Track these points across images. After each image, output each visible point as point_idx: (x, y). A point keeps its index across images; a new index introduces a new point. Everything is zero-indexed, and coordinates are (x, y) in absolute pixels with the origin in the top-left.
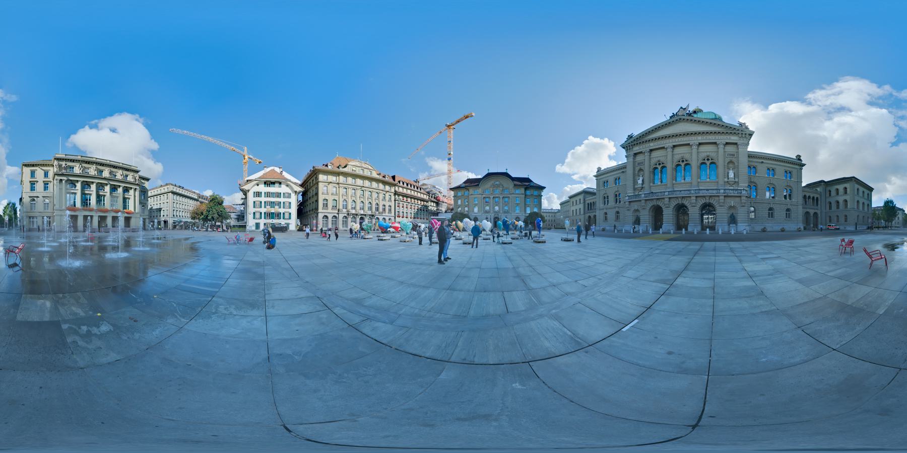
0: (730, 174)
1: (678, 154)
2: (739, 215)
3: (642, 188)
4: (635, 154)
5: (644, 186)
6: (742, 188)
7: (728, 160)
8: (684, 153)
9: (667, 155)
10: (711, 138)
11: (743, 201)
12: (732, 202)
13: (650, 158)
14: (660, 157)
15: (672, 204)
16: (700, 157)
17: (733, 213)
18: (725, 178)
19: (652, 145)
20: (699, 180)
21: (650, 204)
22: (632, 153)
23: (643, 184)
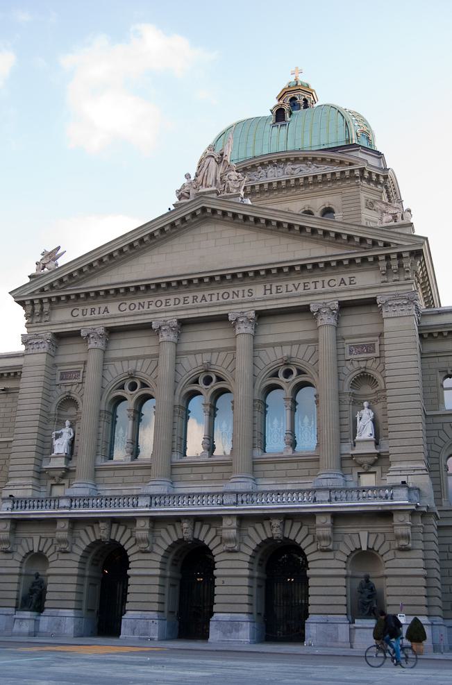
0: (359, 424)
1: (195, 353)
2: (389, 581)
3: (67, 470)
4: (60, 338)
5: (72, 465)
6: (399, 480)
7: (351, 370)
8: (212, 351)
9: (157, 356)
10: (290, 293)
11: (400, 530)
12: (364, 535)
13: (105, 361)
14: (137, 358)
15: (160, 541)
16: (261, 365)
17: (367, 578)
18: (342, 440)
19: (119, 314)
20: (258, 453)
21: (86, 538)
22: (46, 331)
23: (71, 454)
